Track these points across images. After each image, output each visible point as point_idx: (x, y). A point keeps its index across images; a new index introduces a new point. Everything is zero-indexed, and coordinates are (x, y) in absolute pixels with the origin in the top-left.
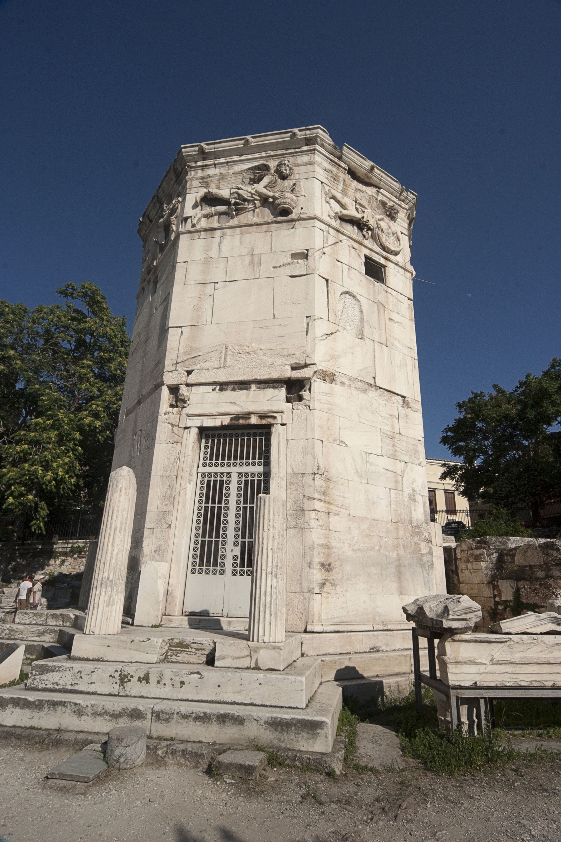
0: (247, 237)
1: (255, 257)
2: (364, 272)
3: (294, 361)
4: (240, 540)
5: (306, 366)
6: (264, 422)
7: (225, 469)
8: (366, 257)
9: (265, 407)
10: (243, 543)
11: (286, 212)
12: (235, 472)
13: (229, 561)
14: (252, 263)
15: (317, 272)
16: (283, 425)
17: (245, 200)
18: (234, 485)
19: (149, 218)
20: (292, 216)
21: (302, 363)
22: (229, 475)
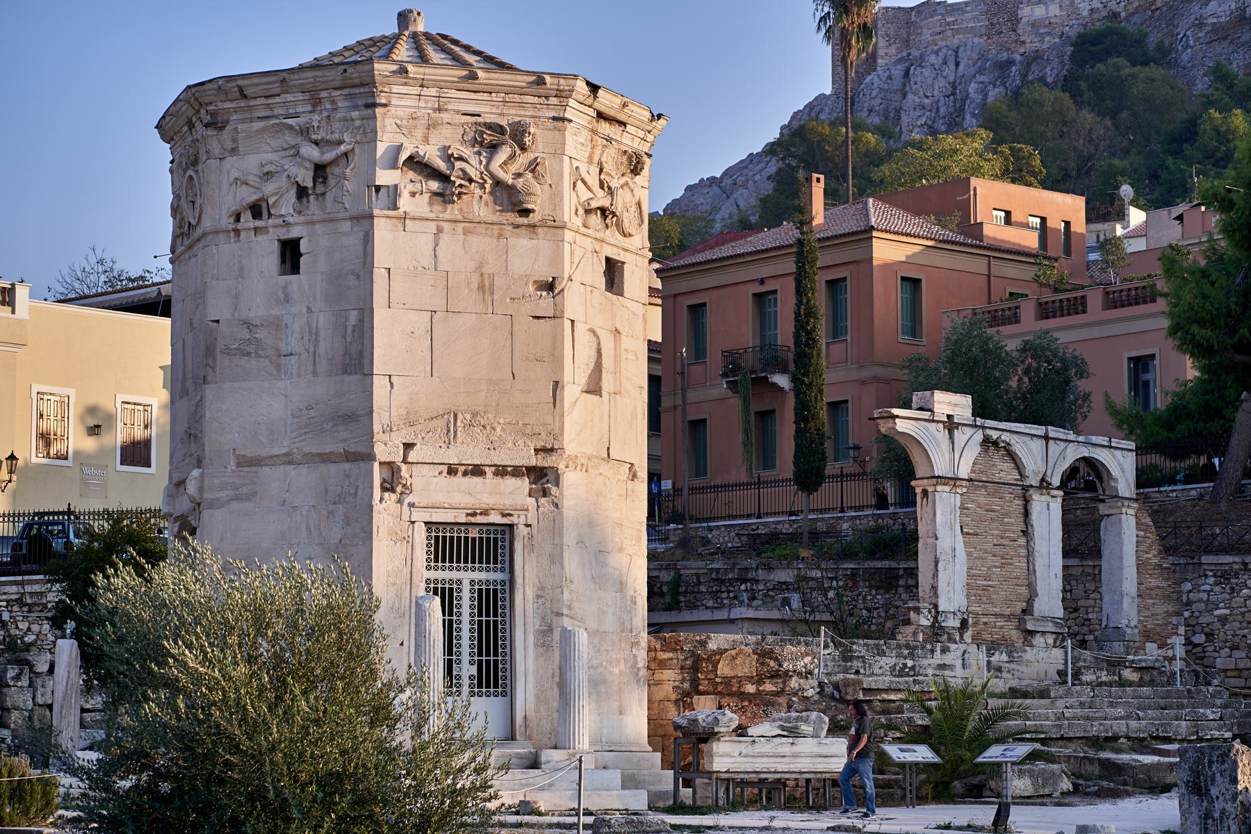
0: (473, 240)
1: (486, 276)
2: (604, 287)
3: (540, 444)
4: (476, 658)
5: (552, 450)
6: (505, 521)
7: (455, 575)
8: (608, 260)
9: (506, 502)
10: (480, 662)
11: (526, 212)
12: (467, 578)
13: (466, 682)
14: (481, 288)
15: (566, 315)
16: (528, 526)
17: (471, 180)
18: (466, 595)
19: (241, 89)
20: (534, 218)
21: (549, 447)
22: (459, 582)
